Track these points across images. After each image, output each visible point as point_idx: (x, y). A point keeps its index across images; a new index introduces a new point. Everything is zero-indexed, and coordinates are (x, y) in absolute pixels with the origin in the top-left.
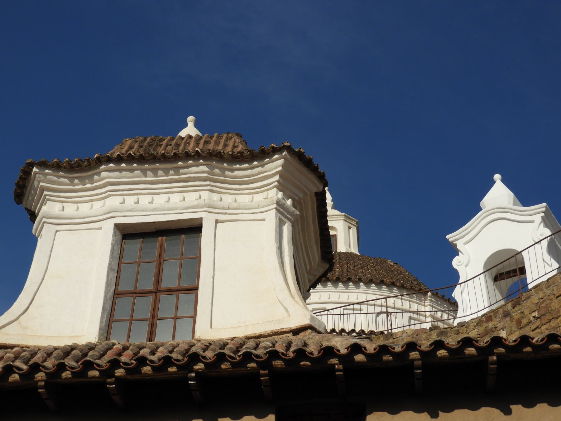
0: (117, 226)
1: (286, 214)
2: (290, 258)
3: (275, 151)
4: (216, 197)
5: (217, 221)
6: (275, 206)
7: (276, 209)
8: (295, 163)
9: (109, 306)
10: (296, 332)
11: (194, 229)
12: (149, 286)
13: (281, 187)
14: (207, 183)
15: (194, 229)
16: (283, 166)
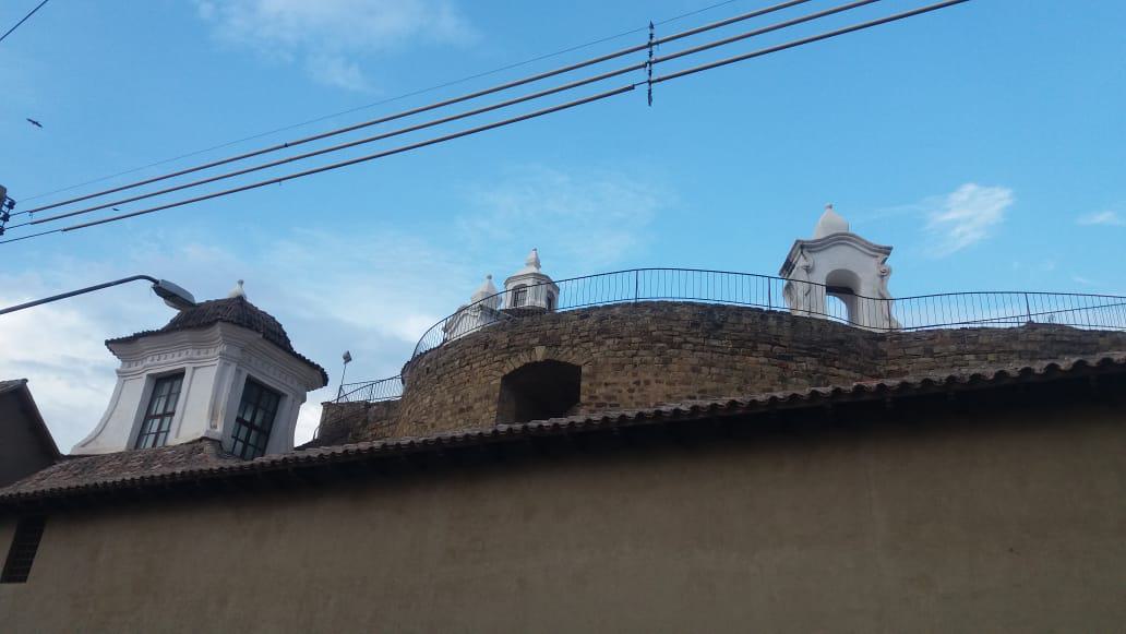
0: (149, 375)
3: (216, 320)
8: (229, 327)
10: (201, 440)
11: (178, 376)
12: (160, 411)
13: (225, 341)
15: (178, 376)
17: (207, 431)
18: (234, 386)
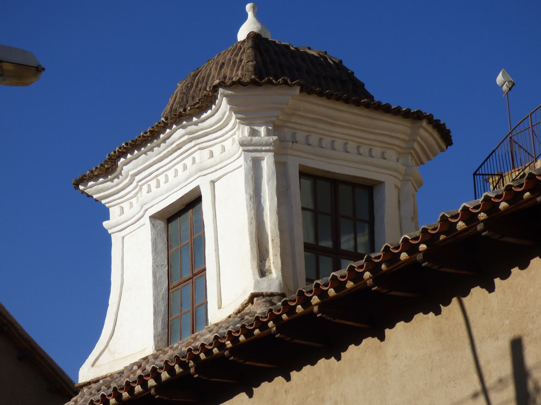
0: (153, 217)
1: (259, 148)
2: (271, 200)
4: (206, 152)
5: (213, 182)
6: (241, 149)
7: (244, 151)
9: (163, 307)
11: (192, 202)
14: (193, 143)
15: (192, 202)
16: (229, 103)
17: (257, 284)
18: (282, 192)
